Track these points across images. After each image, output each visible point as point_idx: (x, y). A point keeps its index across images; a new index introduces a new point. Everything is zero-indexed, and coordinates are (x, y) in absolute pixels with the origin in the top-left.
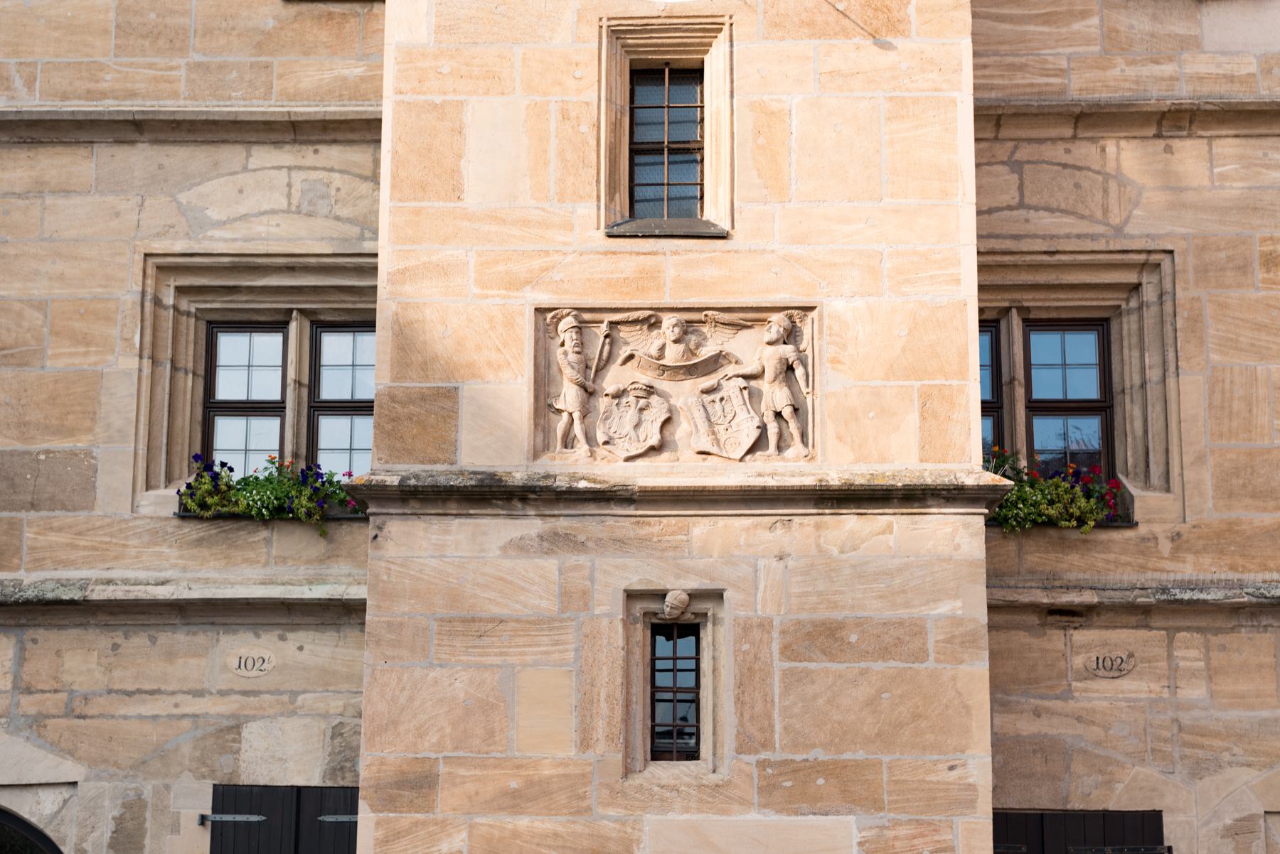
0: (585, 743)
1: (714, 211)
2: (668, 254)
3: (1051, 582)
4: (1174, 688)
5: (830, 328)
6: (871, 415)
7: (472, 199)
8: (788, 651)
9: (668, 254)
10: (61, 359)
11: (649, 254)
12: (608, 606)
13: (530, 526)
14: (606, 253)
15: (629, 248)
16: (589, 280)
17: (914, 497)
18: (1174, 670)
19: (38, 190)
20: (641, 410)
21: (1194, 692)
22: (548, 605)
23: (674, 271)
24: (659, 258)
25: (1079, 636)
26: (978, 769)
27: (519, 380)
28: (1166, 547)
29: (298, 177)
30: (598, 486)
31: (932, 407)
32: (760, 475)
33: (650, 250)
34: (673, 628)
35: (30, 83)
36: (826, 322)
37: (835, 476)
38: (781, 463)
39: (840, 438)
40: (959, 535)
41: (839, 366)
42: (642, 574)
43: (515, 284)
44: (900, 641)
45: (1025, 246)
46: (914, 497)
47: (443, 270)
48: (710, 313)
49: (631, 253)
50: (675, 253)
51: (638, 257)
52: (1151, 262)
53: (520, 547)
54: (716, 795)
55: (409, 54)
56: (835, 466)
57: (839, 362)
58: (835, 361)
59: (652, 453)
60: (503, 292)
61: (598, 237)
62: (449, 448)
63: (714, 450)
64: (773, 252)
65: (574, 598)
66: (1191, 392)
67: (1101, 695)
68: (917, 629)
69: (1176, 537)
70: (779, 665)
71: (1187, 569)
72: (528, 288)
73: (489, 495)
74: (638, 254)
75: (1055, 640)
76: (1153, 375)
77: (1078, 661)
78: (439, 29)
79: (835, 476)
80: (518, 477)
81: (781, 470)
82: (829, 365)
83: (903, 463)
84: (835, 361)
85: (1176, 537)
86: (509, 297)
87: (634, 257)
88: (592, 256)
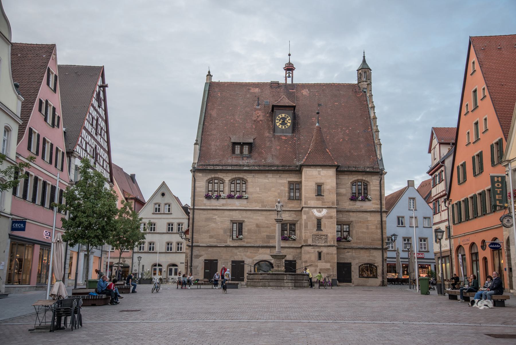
1: (322, 228)
3: (344, 246)
10: (272, 228)
12: (316, 252)
17: (333, 246)
19: (270, 214)
21: (354, 254)
23: (320, 233)
26: (336, 261)
34: (320, 254)
40: (335, 248)
44: (332, 254)
46: (333, 246)
51: (317, 232)
52: (352, 222)
54: (322, 262)
56: (329, 244)
65: (314, 251)
66: (354, 232)
67: (347, 254)
71: (354, 245)
73: (310, 245)
83: (332, 244)
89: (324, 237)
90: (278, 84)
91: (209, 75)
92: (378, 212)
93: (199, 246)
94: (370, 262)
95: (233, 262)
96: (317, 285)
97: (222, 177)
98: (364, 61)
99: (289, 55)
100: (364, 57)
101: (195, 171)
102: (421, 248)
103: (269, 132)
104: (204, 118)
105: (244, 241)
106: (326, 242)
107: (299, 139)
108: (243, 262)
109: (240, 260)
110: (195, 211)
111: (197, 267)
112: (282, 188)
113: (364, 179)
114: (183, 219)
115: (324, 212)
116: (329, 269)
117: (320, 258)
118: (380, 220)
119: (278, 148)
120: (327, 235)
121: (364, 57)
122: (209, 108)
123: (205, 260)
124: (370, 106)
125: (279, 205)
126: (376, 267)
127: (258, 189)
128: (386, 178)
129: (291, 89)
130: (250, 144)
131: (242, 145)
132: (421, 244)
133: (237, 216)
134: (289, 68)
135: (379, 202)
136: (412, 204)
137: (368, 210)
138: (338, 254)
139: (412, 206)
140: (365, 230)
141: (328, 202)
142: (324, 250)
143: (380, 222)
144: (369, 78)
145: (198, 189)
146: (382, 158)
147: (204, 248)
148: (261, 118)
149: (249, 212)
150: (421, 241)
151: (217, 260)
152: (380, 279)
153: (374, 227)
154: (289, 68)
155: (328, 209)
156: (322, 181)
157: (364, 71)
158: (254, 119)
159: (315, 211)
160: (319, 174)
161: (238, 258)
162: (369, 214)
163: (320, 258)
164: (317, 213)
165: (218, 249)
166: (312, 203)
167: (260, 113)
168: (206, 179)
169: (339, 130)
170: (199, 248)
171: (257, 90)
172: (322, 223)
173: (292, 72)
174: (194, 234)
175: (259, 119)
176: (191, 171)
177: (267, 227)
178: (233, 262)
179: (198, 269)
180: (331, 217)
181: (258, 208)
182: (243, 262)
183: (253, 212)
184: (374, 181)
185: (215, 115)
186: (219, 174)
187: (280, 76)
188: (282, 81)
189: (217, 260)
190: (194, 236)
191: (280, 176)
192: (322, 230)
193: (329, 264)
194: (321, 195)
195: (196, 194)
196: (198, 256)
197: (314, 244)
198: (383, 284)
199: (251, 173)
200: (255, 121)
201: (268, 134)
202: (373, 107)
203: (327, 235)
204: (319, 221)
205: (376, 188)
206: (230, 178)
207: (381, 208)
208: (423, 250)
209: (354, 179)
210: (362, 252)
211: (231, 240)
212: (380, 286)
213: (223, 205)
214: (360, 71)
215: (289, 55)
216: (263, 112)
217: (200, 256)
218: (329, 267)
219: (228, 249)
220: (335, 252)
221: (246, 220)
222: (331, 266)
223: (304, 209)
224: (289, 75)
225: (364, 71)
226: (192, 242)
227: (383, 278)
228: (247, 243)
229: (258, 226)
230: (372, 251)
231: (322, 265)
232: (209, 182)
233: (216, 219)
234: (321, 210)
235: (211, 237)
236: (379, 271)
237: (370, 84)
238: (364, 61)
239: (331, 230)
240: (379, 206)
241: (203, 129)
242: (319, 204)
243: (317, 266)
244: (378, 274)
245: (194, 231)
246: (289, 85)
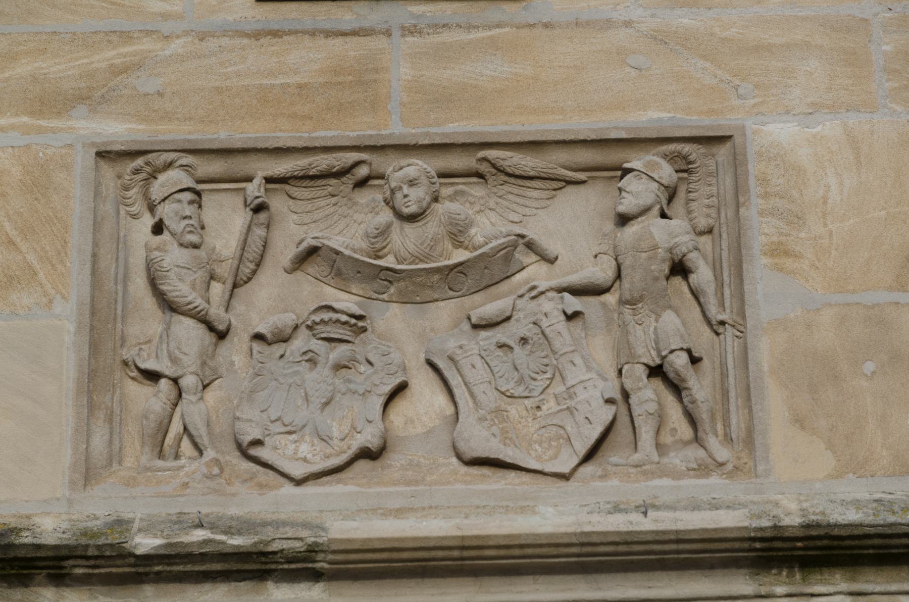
2: (396, 33)
5: (764, 181)
6: (869, 367)
9: (396, 33)
11: (354, 33)
14: (257, 35)
15: (309, 24)
16: (219, 90)
20: (339, 367)
24: (378, 43)
27: (59, 307)
30: (237, 541)
32: (617, 509)
33: (356, 25)
36: (754, 168)
37: (793, 506)
38: (666, 482)
39: (800, 421)
41: (789, 263)
43: (51, 102)
48: (492, 154)
49: (313, 33)
50: (412, 30)
57: (787, 253)
58: (778, 250)
59: (363, 465)
60: (25, 119)
63: (508, 454)
64: (628, 24)
72: (82, 109)
74: (329, 34)
79: (793, 506)
80: (50, 527)
81: (666, 498)
82: (765, 260)
84: (778, 250)
86: (40, 131)
87: (321, 41)
88: (225, 41)
89: (571, 230)
120: (697, 152)
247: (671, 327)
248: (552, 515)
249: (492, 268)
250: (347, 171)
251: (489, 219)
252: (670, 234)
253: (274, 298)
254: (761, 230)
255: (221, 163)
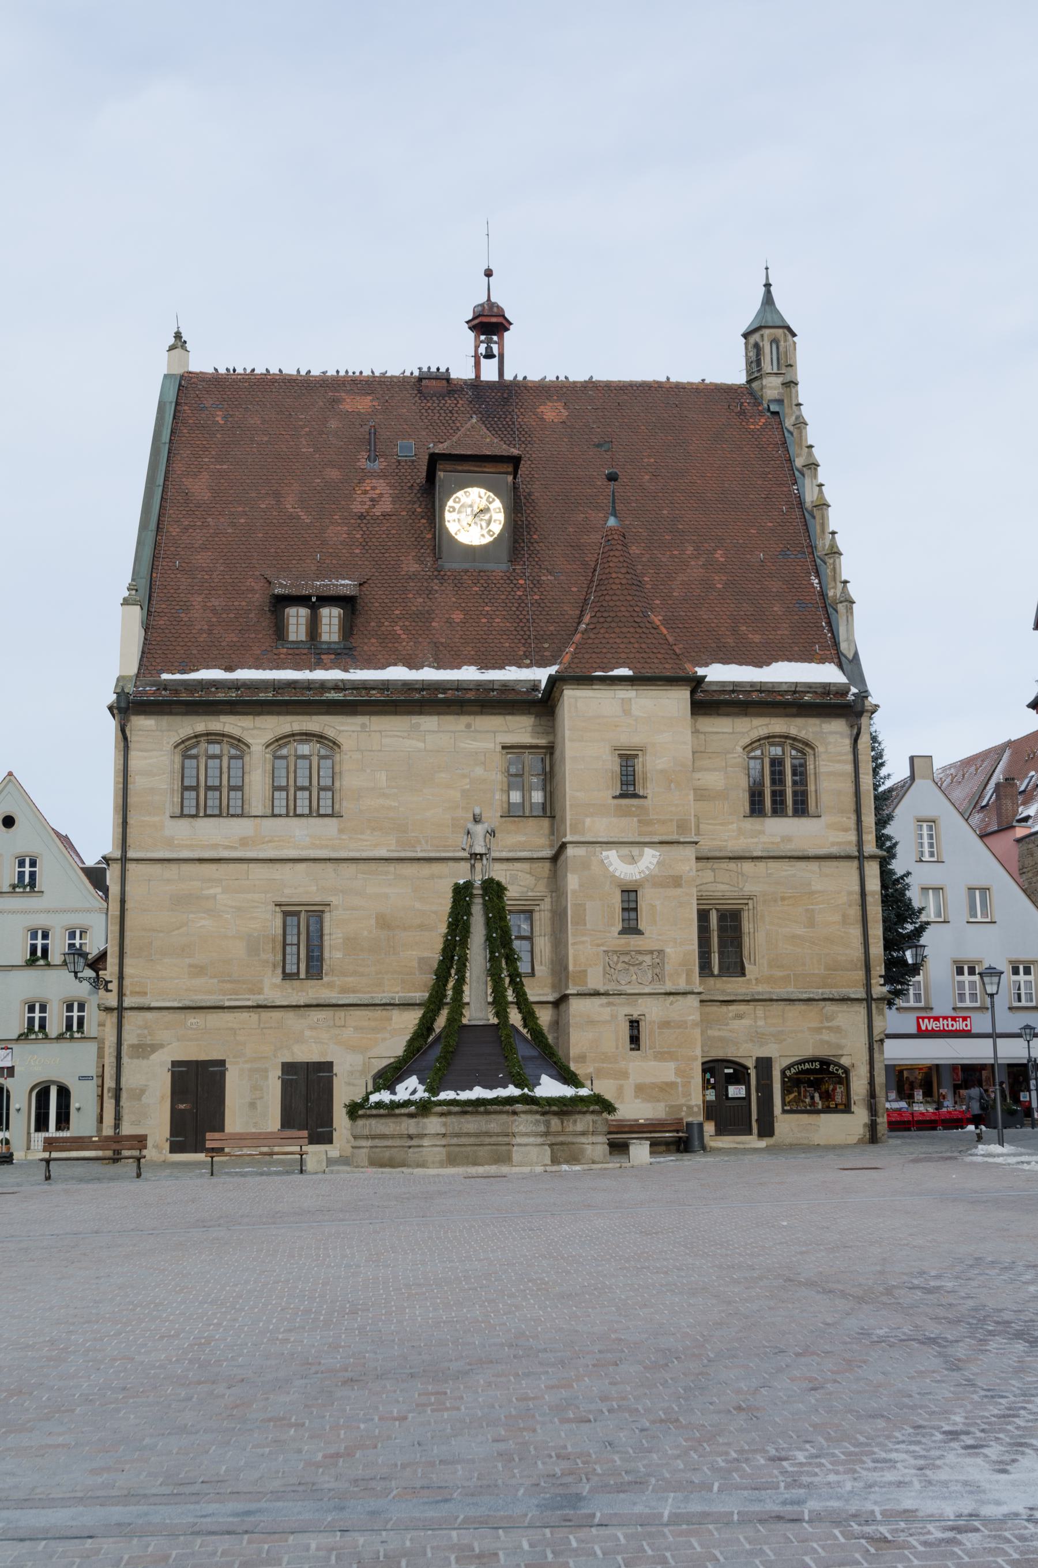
0: (617, 1048)
1: (642, 926)
4: (755, 1022)
7: (588, 926)
8: (659, 1028)
13: (604, 1000)
18: (756, 1017)
19: (432, 877)
21: (761, 1023)
22: (608, 1018)
23: (634, 941)
25: (731, 1008)
26: (698, 1052)
28: (754, 982)
29: (508, 873)
31: (689, 973)
35: (427, 842)
42: (628, 1010)
43: (598, 945)
44: (682, 1025)
45: (716, 894)
47: (583, 942)
53: (602, 1005)
55: (574, 892)
56: (669, 987)
61: (616, 934)
62: (585, 984)
65: (614, 1017)
67: (736, 1024)
68: (685, 1022)
69: (757, 979)
70: (657, 1031)
71: (760, 988)
73: (596, 994)
75: (724, 1008)
76: (752, 930)
77: (730, 1015)
78: (580, 886)
80: (602, 991)
83: (682, 985)
85: (757, 979)
89: (647, 959)
90: (448, 380)
91: (179, 342)
92: (849, 857)
93: (149, 1009)
94: (823, 1052)
95: (288, 1068)
96: (640, 1152)
97: (236, 732)
98: (768, 300)
99: (489, 273)
100: (768, 285)
101: (127, 707)
102: (962, 997)
103: (419, 560)
104: (161, 507)
105: (330, 986)
106: (659, 977)
107: (537, 583)
108: (327, 1067)
109: (315, 1058)
110: (130, 866)
111: (142, 1091)
112: (479, 771)
113: (793, 731)
114: (89, 911)
115: (649, 859)
116: (672, 1085)
117: (635, 1040)
118: (857, 888)
119: (458, 616)
120: (661, 952)
121: (768, 285)
122: (178, 467)
123: (174, 1064)
124: (799, 462)
125: (479, 830)
126: (846, 1071)
127: (382, 777)
128: (879, 724)
129: (500, 400)
130: (346, 602)
131: (314, 603)
132: (961, 984)
133: (301, 886)
134: (489, 324)
135: (852, 822)
136: (926, 841)
137: (811, 852)
138: (706, 1022)
139: (926, 849)
140: (800, 931)
141: (663, 822)
142: (652, 1011)
143: (857, 897)
144: (786, 363)
145: (137, 783)
146: (856, 655)
147: (168, 1016)
148: (386, 506)
149: (351, 869)
150: (960, 971)
151: (222, 1063)
152: (860, 1115)
153: (837, 918)
154: (489, 324)
155: (666, 848)
156: (636, 740)
157: (769, 336)
158: (357, 508)
159: (612, 858)
160: (627, 712)
161: (307, 1053)
162: (814, 866)
163: (635, 1040)
164: (621, 867)
165: (228, 1017)
166: (599, 827)
167: (381, 487)
168: (176, 739)
169: (690, 550)
170: (149, 1015)
171: (364, 404)
172: (643, 906)
173: (501, 338)
174: (127, 961)
175: (377, 511)
176: (111, 708)
177: (422, 927)
178: (288, 1068)
179: (144, 1099)
180: (676, 881)
181: (383, 853)
182: (328, 1066)
183: (362, 866)
184: (831, 739)
185: (207, 495)
186: (223, 718)
187: (457, 357)
188: (462, 371)
189: (222, 1063)
190: (127, 970)
191: (468, 726)
192: (640, 933)
193: (672, 1065)
194: (635, 796)
195: (131, 800)
196: (144, 1050)
197: (611, 987)
198: (873, 1137)
199: (354, 713)
200: (362, 517)
201: (414, 567)
202: (813, 466)
203: (661, 952)
204: (630, 895)
205: (838, 767)
206: (269, 737)
207: (860, 843)
208: (968, 1003)
209: (755, 735)
210: (793, 1012)
211: (278, 979)
212: (861, 1141)
213: (244, 842)
214: (756, 337)
215: (489, 273)
216: (392, 486)
217: (154, 1048)
218: (672, 1078)
219: (266, 1015)
220: (695, 1017)
221: (335, 900)
222: (679, 1072)
223: (570, 851)
224: (489, 349)
225: (769, 336)
226: (121, 995)
227: (873, 1110)
228: (344, 990)
229: (384, 922)
230: (830, 1008)
231: (644, 1068)
232: (186, 748)
233: (214, 897)
234: (635, 851)
235: (199, 970)
236: (859, 1086)
237: (791, 384)
238: (768, 300)
239: (673, 933)
240: (852, 837)
241: (156, 545)
242: (625, 827)
243: (624, 1075)
244: (854, 1097)
245: (127, 949)
246: (490, 385)
247: (657, 971)
248: (647, 990)
249: (640, 964)
250: (627, 953)
251: (641, 958)
252: (658, 960)
253: (620, 966)
254: (666, 960)
255: (616, 952)
